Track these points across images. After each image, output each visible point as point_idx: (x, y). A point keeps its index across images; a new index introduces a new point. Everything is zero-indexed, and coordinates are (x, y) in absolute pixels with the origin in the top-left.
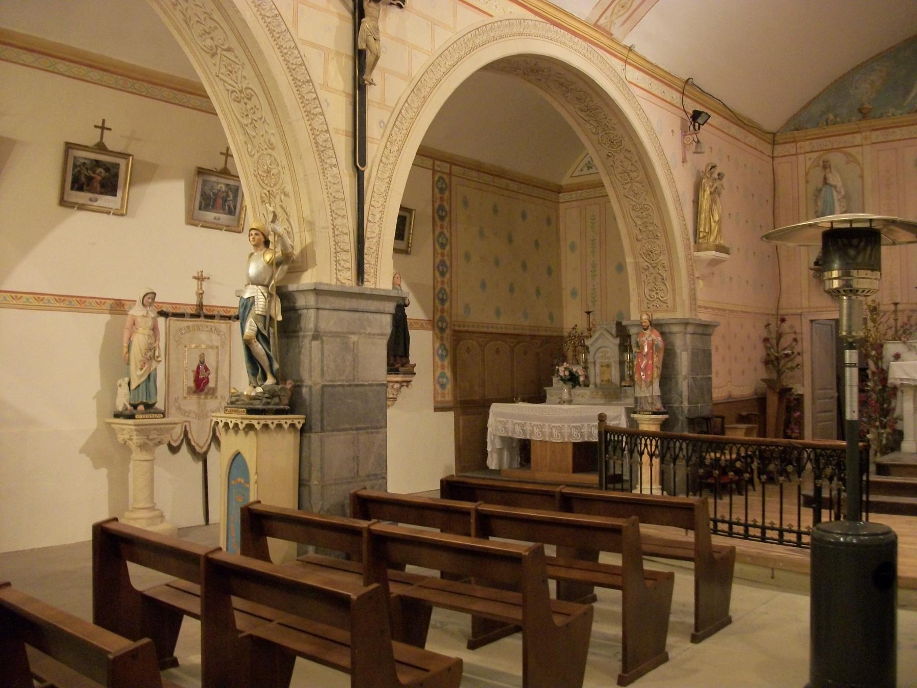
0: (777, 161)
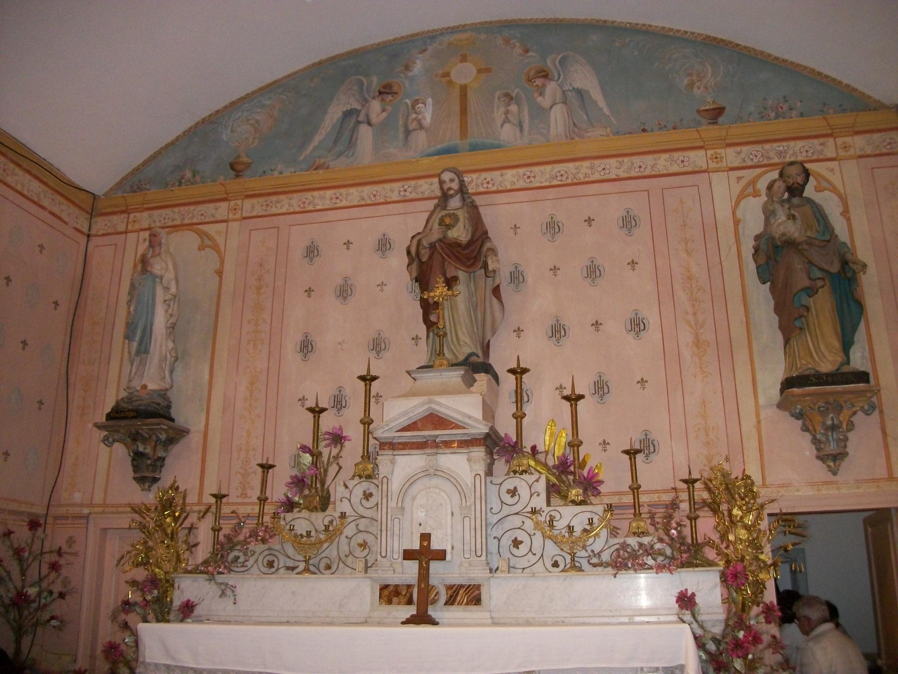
0: (94, 241)
